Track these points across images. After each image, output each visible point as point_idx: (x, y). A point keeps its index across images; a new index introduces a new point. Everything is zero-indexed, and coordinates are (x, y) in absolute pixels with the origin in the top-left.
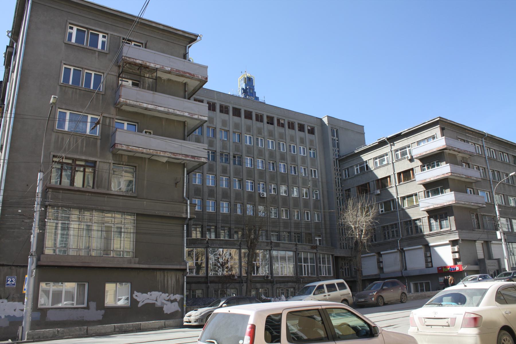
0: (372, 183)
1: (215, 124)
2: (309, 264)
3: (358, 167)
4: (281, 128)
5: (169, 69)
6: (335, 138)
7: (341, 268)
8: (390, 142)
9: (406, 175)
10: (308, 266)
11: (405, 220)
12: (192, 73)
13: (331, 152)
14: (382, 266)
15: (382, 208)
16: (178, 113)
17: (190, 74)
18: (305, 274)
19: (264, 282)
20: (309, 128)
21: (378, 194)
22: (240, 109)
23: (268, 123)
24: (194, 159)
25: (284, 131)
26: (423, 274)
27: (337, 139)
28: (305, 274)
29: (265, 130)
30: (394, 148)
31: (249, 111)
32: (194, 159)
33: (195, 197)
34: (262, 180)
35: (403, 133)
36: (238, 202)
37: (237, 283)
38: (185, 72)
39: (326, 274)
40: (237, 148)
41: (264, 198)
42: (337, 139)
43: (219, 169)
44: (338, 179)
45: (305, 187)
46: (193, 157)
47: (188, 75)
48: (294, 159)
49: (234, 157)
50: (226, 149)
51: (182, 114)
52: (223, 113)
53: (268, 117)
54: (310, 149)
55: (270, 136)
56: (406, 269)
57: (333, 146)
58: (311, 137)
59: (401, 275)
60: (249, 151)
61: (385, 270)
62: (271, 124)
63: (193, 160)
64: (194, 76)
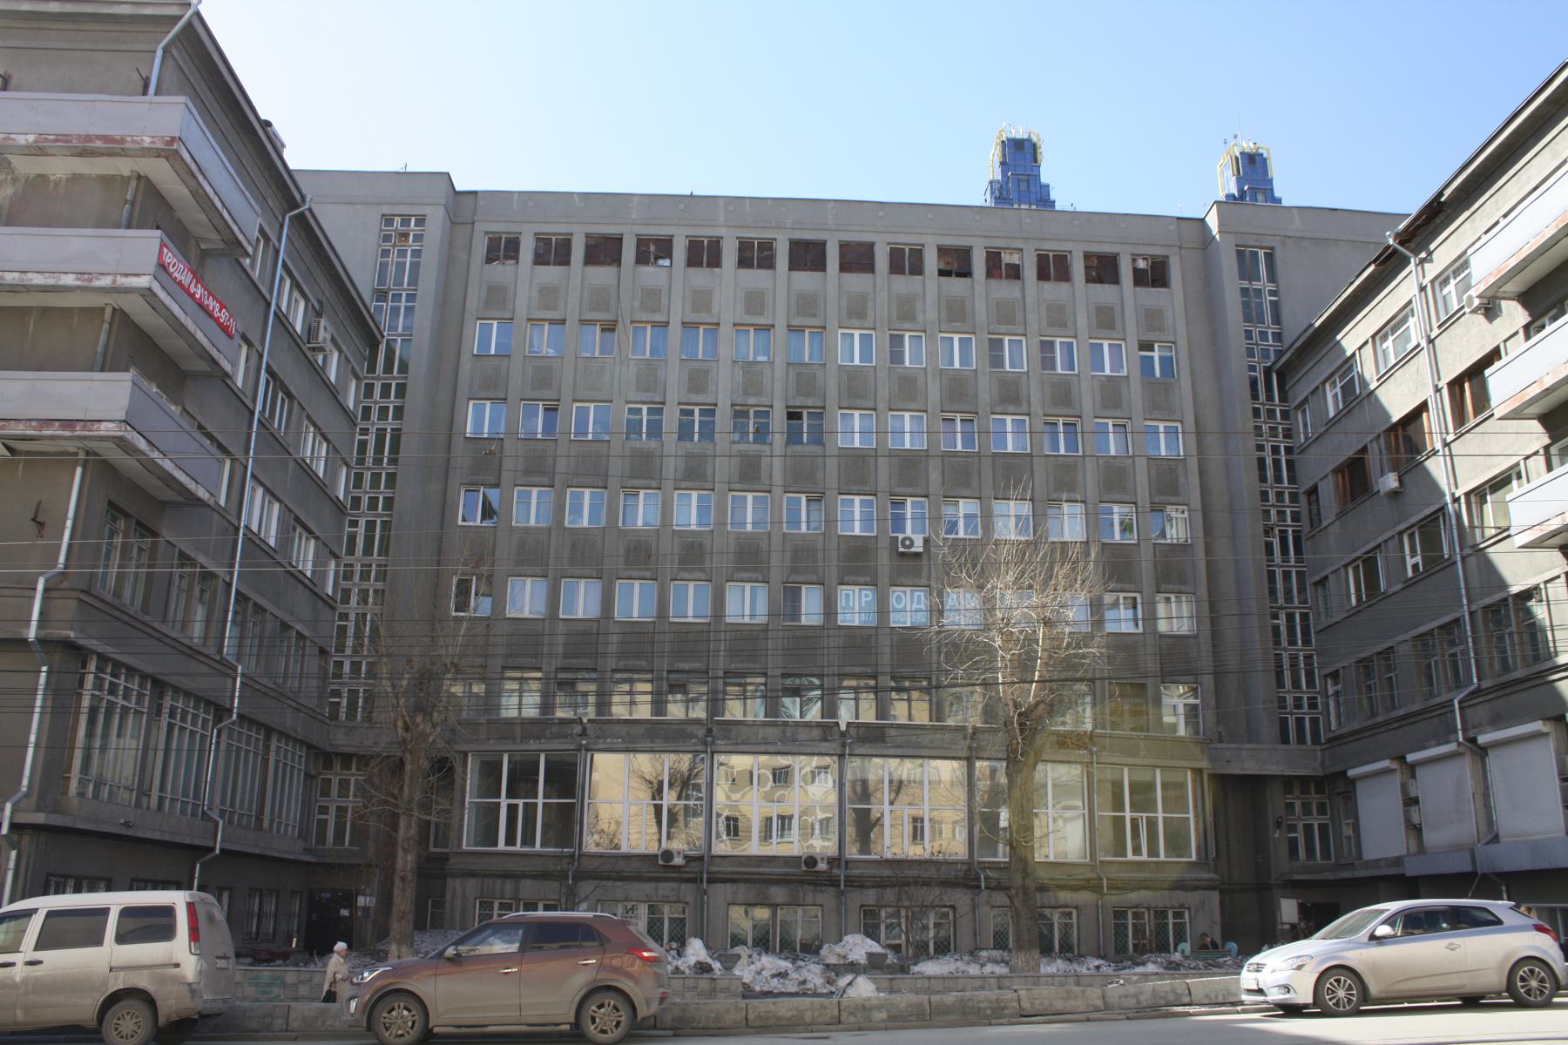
0: (1375, 444)
1: (715, 310)
2: (1160, 815)
3: (1338, 389)
4: (1004, 283)
5: (31, 138)
6: (1263, 284)
7: (1278, 825)
8: (1416, 253)
9: (1470, 386)
10: (1152, 824)
11: (1488, 601)
12: (116, 132)
13: (1237, 343)
14: (1416, 820)
15: (1413, 553)
16: (38, 280)
17: (106, 139)
18: (1137, 850)
19: (801, 882)
20: (1141, 264)
21: (1394, 494)
22: (871, 246)
23: (942, 273)
24: (73, 428)
25: (1017, 294)
26: (1545, 865)
27: (1271, 287)
28: (1137, 850)
29: (929, 299)
30: (1432, 270)
31: (860, 244)
32: (73, 428)
33: (626, 574)
34: (911, 490)
35: (1447, 193)
36: (801, 578)
37: (689, 880)
38: (88, 138)
39: (1153, 851)
40: (805, 378)
41: (917, 555)
42: (1271, 287)
43: (723, 468)
44: (1275, 450)
45: (1118, 497)
46: (68, 423)
47: (98, 144)
48: (1063, 394)
49: (794, 416)
50: (759, 393)
51: (51, 281)
52: (751, 266)
53: (943, 251)
54: (1146, 346)
55: (951, 320)
56: (1496, 839)
57: (1248, 318)
58: (1152, 296)
59: (1469, 868)
60: (857, 390)
61: (1430, 838)
62: (959, 275)
63: (67, 433)
64: (122, 141)
